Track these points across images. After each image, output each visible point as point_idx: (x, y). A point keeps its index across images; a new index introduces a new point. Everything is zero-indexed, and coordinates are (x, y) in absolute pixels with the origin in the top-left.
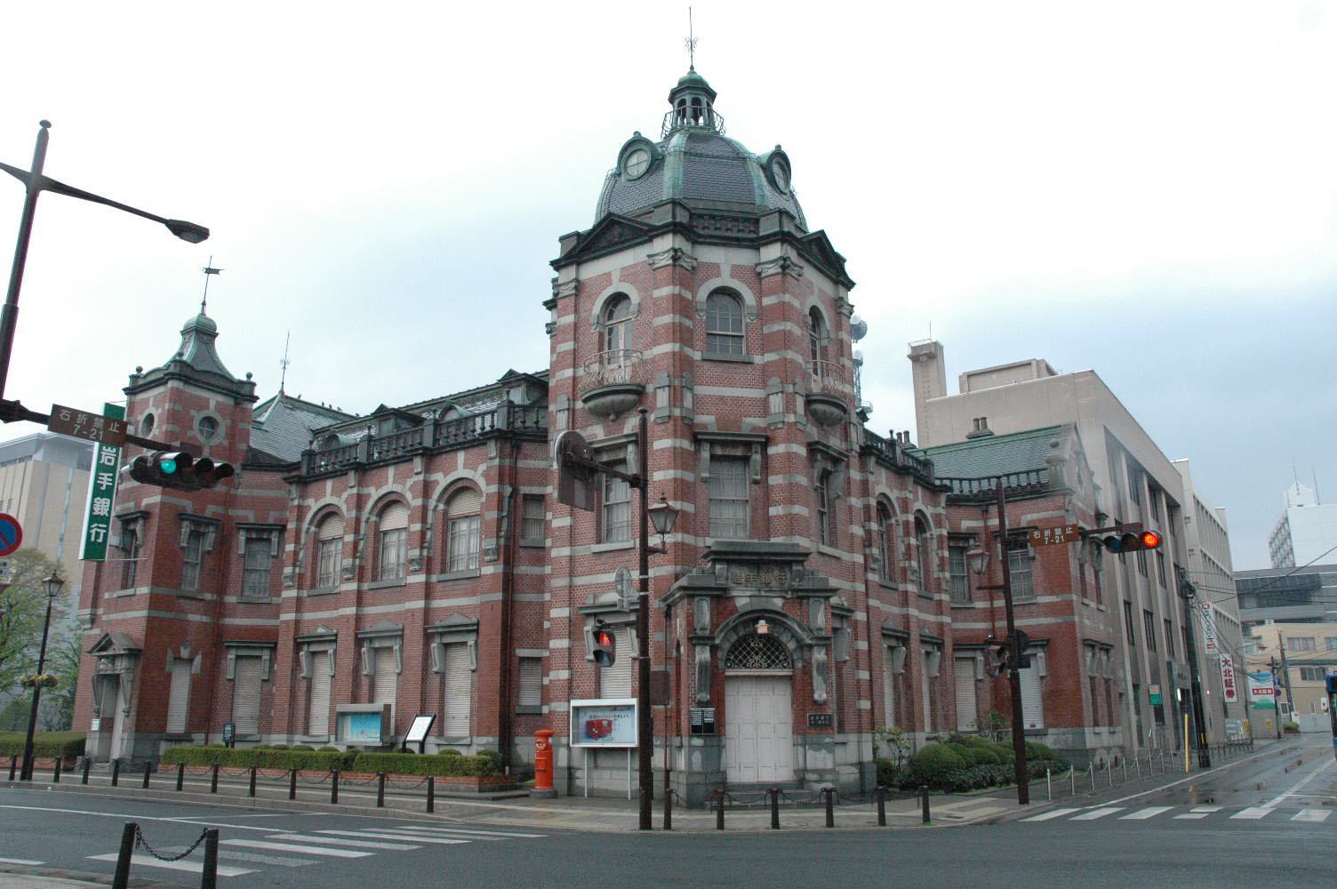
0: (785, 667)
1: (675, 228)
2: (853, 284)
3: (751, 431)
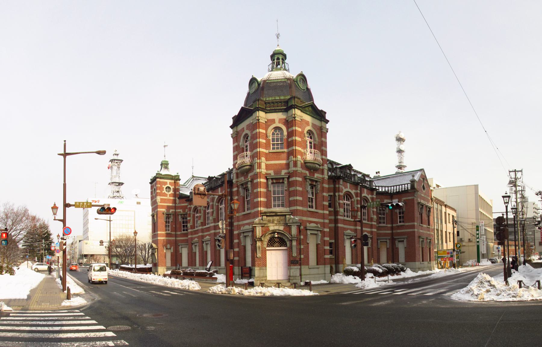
0: (286, 247)
3: (285, 174)
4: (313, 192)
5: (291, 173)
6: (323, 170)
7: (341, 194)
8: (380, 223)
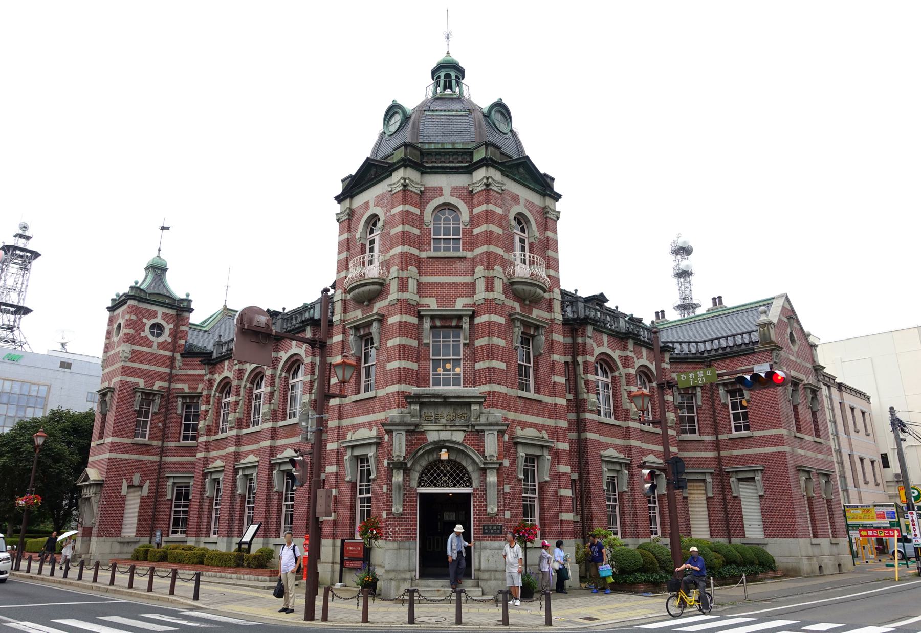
0: (468, 486)
1: (405, 163)
2: (561, 196)
3: (463, 307)
4: (529, 353)
5: (479, 305)
6: (551, 301)
7: (591, 359)
8: (684, 432)
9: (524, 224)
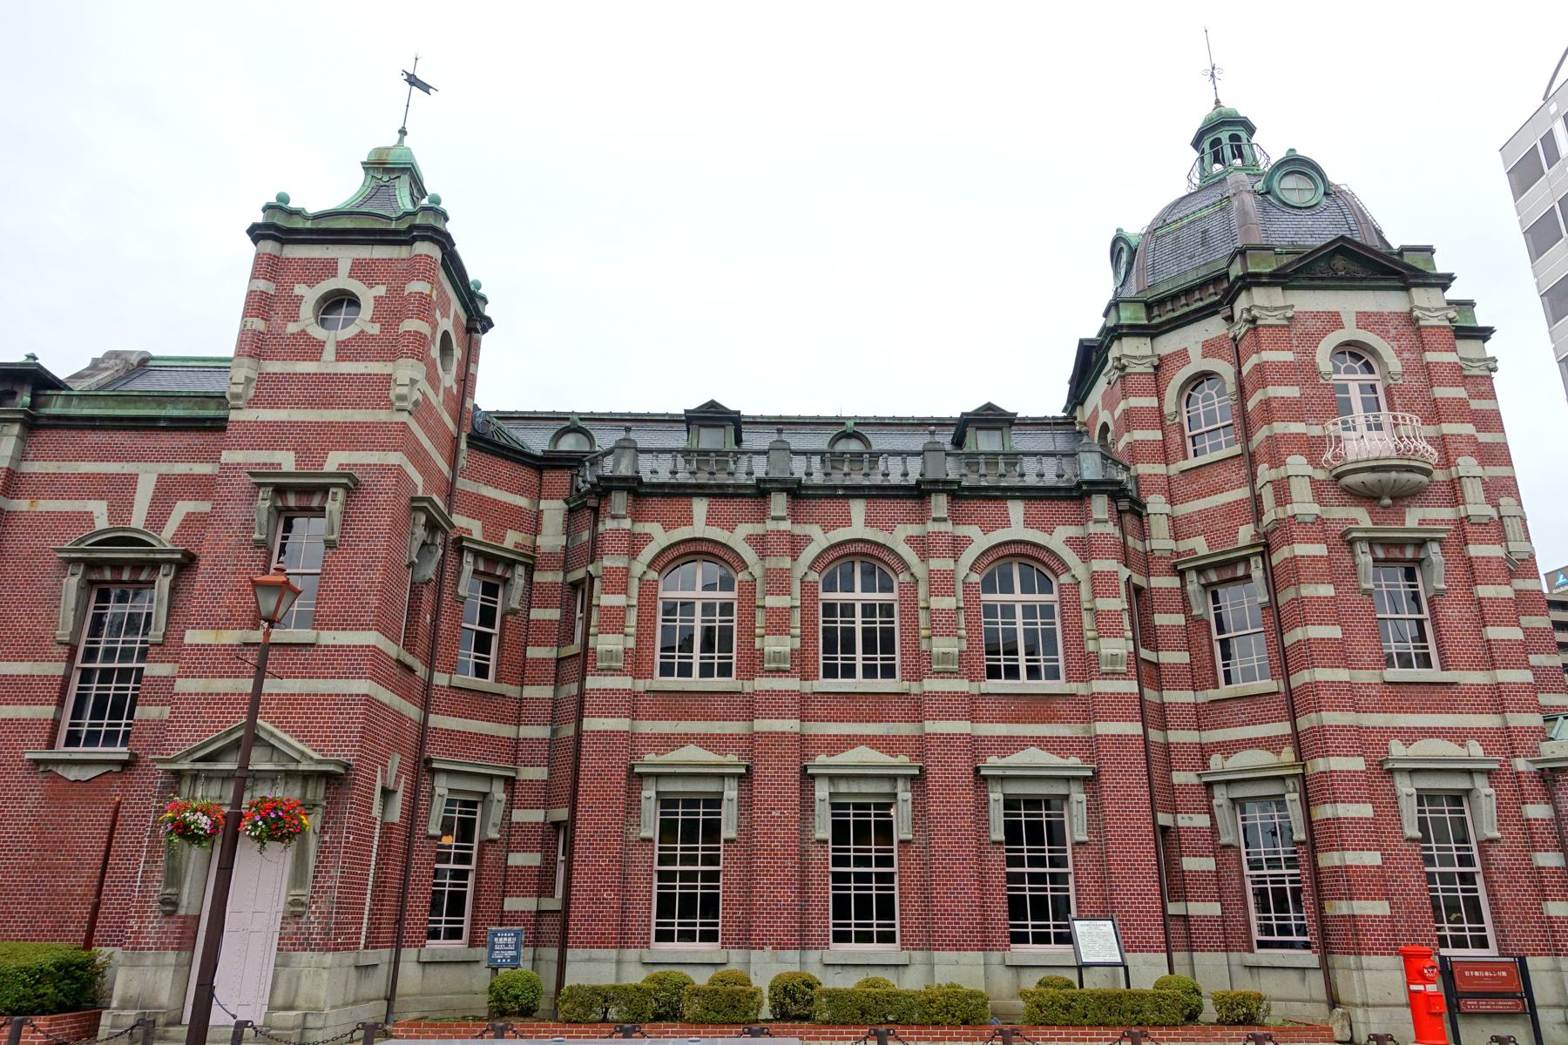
9: (1368, 357)
